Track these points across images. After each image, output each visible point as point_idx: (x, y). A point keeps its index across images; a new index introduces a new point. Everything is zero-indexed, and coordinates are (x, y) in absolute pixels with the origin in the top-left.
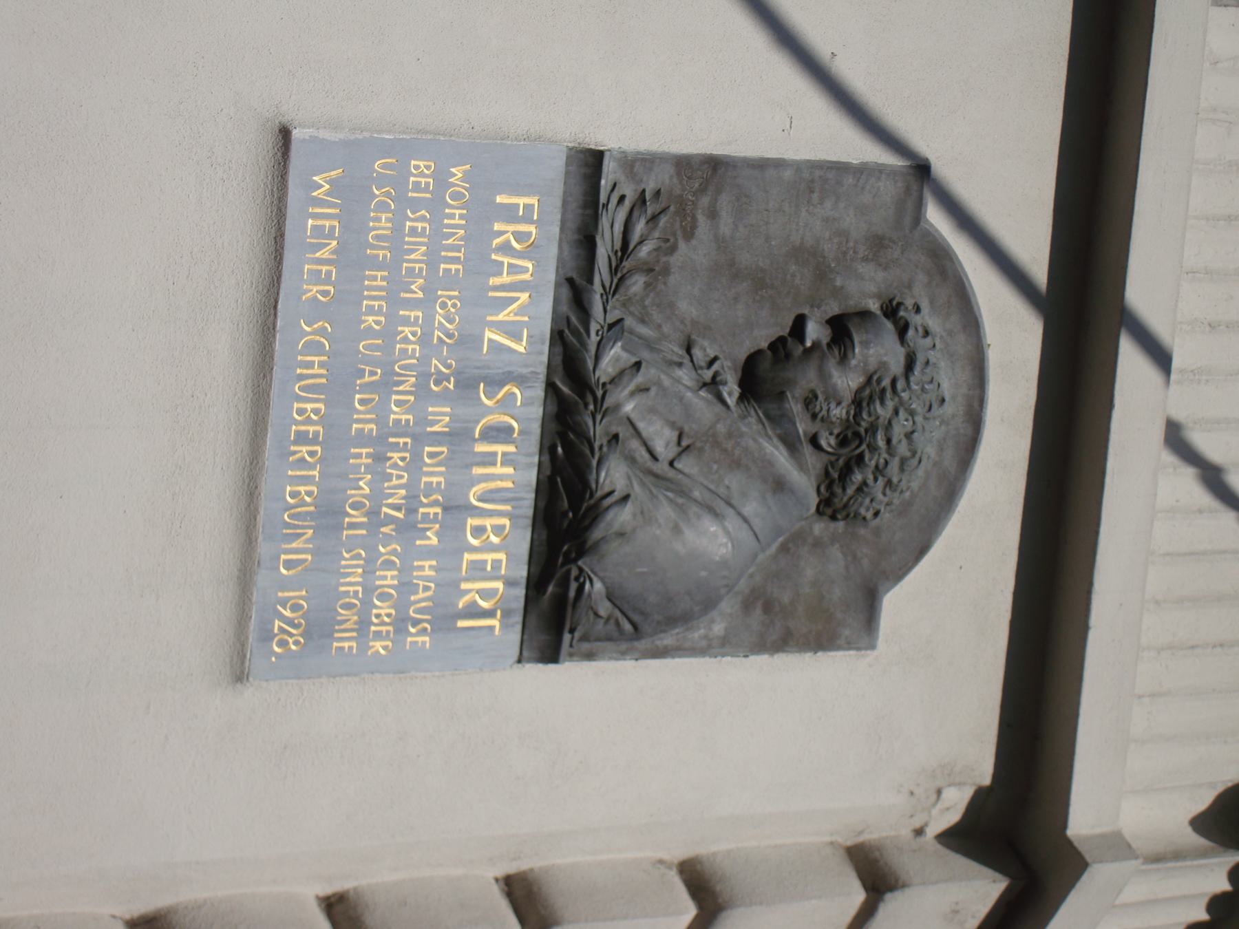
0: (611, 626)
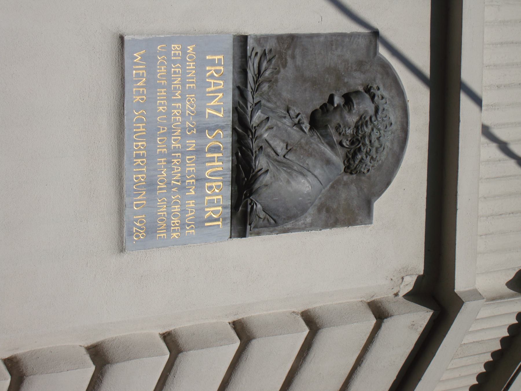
0: (266, 221)
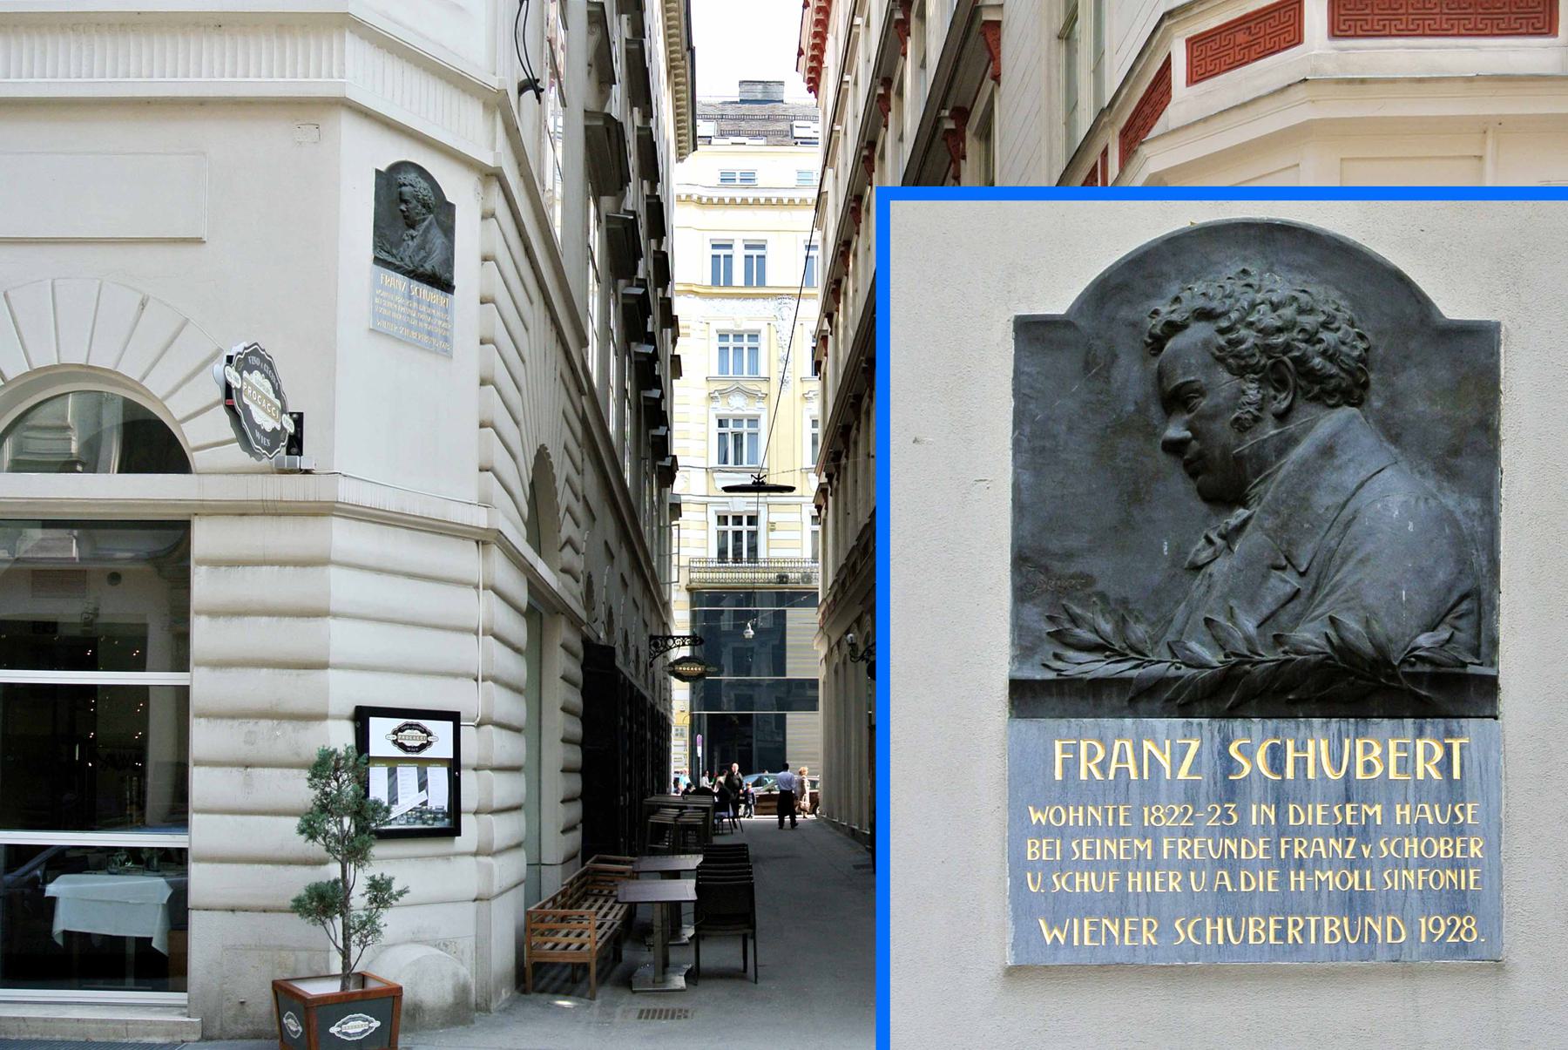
0: (1462, 623)
